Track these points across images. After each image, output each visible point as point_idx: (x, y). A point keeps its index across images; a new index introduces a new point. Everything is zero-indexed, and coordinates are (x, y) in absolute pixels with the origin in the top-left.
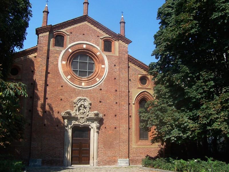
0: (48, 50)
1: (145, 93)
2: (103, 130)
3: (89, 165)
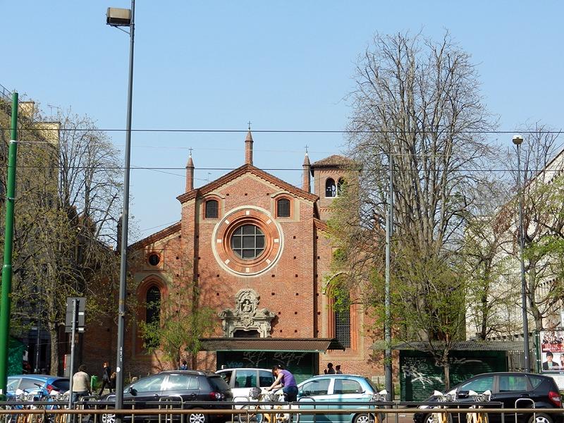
0: (197, 225)
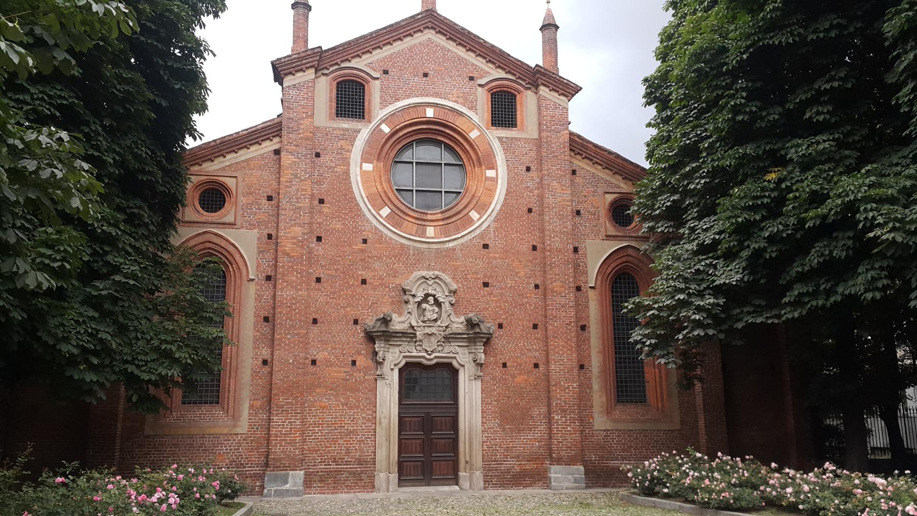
1: (631, 252)
2: (498, 371)
3: (457, 488)
